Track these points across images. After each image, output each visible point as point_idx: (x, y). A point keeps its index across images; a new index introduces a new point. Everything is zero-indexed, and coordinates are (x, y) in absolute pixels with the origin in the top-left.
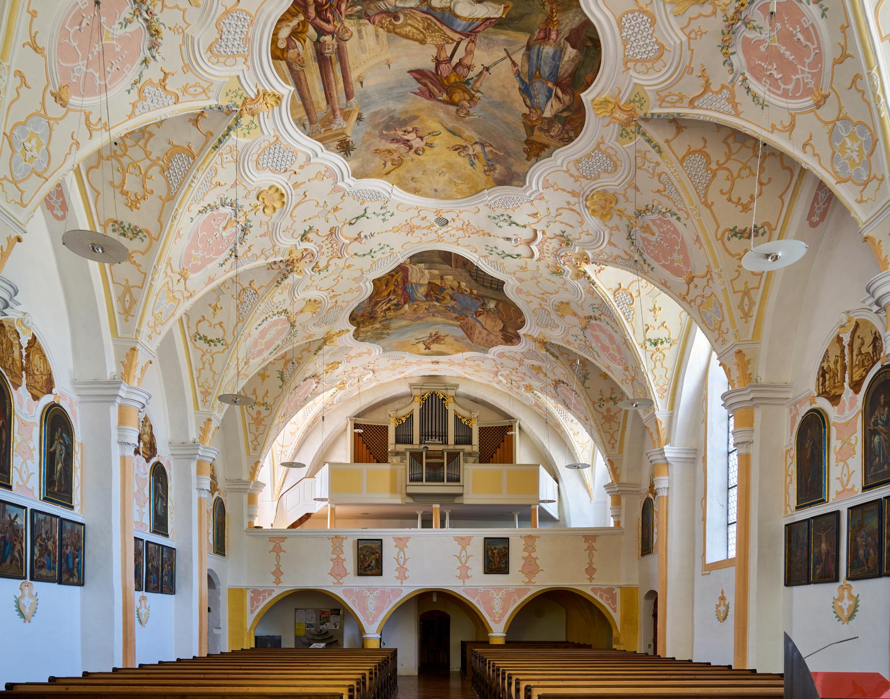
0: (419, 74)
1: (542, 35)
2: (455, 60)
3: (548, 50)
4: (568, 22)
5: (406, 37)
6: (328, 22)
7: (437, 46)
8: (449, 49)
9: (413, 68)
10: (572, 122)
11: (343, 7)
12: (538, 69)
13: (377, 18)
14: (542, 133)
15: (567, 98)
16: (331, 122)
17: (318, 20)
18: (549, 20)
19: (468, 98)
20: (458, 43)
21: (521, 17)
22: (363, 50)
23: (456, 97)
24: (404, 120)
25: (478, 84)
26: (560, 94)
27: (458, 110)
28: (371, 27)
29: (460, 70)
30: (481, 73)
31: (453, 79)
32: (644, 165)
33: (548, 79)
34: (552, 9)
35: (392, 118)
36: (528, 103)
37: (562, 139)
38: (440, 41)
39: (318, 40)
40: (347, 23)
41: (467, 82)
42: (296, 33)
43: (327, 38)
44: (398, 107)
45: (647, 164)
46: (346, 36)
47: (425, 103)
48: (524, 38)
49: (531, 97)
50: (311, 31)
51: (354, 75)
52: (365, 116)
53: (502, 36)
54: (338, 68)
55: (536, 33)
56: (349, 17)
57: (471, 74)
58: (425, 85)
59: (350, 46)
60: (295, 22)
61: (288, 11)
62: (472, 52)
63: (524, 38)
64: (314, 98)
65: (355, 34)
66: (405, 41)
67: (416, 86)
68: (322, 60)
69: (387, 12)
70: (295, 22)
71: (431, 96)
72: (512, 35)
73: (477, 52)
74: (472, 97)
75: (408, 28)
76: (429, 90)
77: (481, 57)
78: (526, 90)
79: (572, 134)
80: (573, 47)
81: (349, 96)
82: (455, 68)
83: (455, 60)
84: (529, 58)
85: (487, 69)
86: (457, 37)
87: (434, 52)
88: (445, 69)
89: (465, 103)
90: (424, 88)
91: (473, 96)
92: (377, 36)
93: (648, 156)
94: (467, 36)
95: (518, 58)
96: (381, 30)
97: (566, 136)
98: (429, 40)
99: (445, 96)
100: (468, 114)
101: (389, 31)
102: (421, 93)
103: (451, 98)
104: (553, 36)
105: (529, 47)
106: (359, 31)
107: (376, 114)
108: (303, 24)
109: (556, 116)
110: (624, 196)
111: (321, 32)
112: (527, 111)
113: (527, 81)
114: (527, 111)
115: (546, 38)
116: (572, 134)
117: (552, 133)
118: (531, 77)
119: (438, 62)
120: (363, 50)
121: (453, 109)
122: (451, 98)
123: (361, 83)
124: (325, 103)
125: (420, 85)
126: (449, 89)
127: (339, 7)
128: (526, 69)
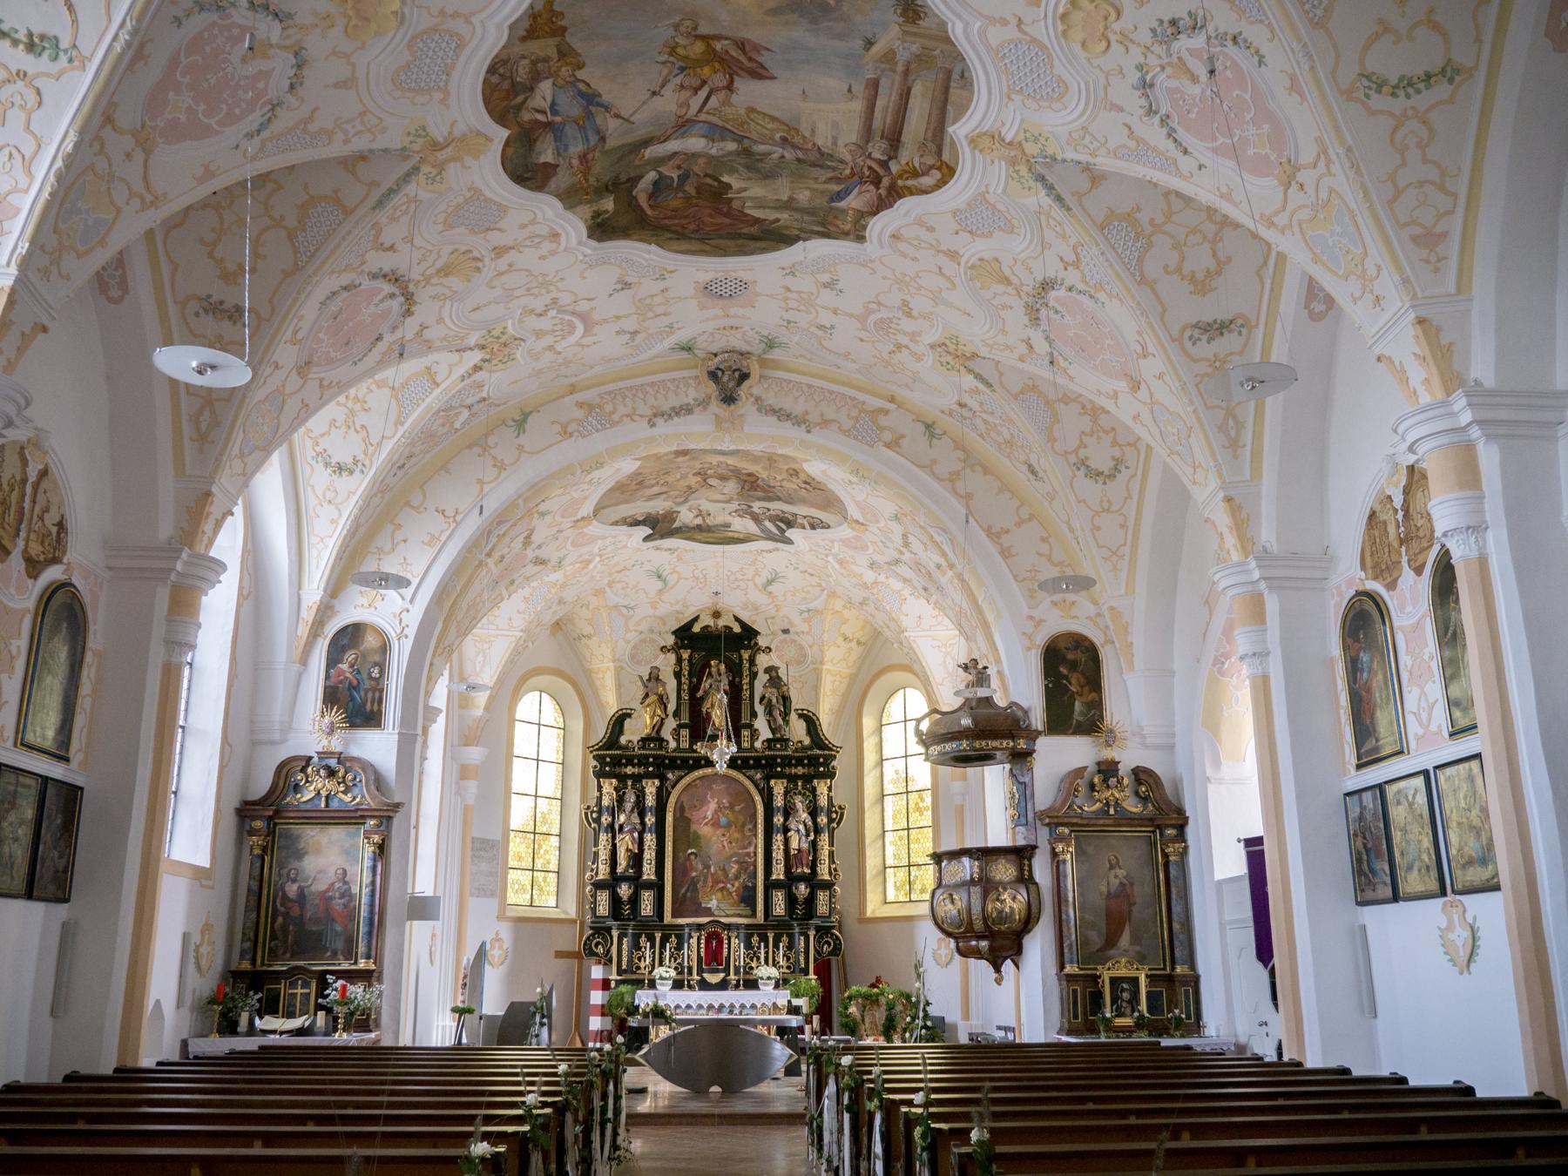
0: (759, 73)
1: (590, 156)
2: (703, 93)
3: (576, 149)
4: (562, 179)
5: (773, 119)
6: (870, 168)
7: (731, 105)
8: (713, 101)
9: (768, 83)
10: (504, 91)
11: (848, 172)
12: (582, 128)
13: (809, 146)
14: (542, 54)
15: (526, 116)
16: (918, 58)
17: (881, 172)
18: (586, 172)
19: (680, 51)
20: (700, 111)
21: (620, 159)
22: (835, 125)
23: (699, 47)
24: (793, 12)
25: (665, 72)
26: (540, 117)
27: (695, 28)
28: (820, 142)
29: (696, 82)
30: (663, 86)
31: (706, 70)
32: (362, 123)
33: (563, 124)
34: (587, 180)
35: (814, 21)
36: (582, 86)
37: (504, 62)
38: (727, 109)
39: (890, 158)
40: (848, 158)
41: (682, 69)
42: (915, 174)
43: (877, 155)
44: (799, 33)
45: (359, 127)
46: (853, 148)
47: (753, 34)
48: (611, 143)
49: (581, 94)
50: (894, 168)
51: (858, 106)
52: (858, 44)
53: (641, 133)
54: (877, 123)
55: (597, 154)
56: (842, 162)
57: (678, 80)
58: (750, 59)
59: (850, 134)
60: (910, 183)
61: (912, 194)
62: (681, 106)
63: (611, 143)
64: (927, 106)
65: (841, 143)
66: (777, 114)
67: (765, 59)
68: (894, 140)
69: (795, 147)
70: (910, 183)
71: (741, 45)
72: (629, 140)
73: (673, 108)
74: (673, 51)
75: (770, 126)
76: (744, 51)
77: (668, 103)
78: (590, 99)
79: (494, 79)
80: (546, 164)
81: (874, 85)
82: (704, 83)
83: (703, 93)
84: (598, 132)
85: (654, 93)
86: (703, 117)
87: (734, 98)
88: (720, 80)
89: (681, 41)
90: (755, 56)
91: (671, 54)
92: (813, 131)
93: (368, 136)
94: (688, 121)
95: (612, 124)
96: (807, 135)
97: (501, 71)
98: (742, 111)
99: (718, 46)
100: (677, 27)
101: (797, 131)
102: (757, 48)
103: (709, 45)
104: (575, 162)
105: (603, 139)
106: (835, 143)
107: (840, 37)
108: (900, 177)
109: (532, 89)
110: (347, 56)
111: (884, 164)
112: (580, 74)
113: (593, 109)
114: (580, 74)
115: (583, 158)
116: (494, 79)
117: (526, 62)
118: (589, 115)
119: (730, 87)
120: (835, 125)
121: (704, 29)
122: (709, 45)
123: (850, 90)
124: (913, 91)
125: (759, 59)
126: (712, 57)
127: (853, 174)
128: (599, 120)
